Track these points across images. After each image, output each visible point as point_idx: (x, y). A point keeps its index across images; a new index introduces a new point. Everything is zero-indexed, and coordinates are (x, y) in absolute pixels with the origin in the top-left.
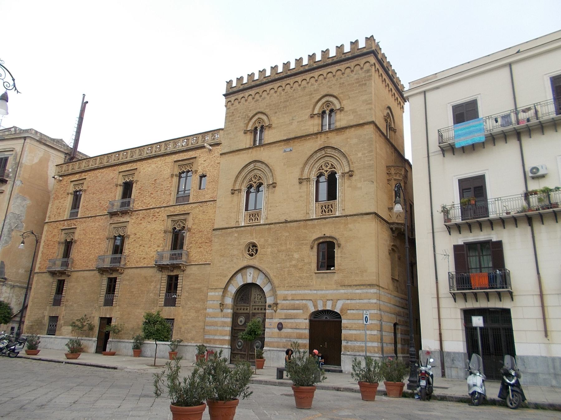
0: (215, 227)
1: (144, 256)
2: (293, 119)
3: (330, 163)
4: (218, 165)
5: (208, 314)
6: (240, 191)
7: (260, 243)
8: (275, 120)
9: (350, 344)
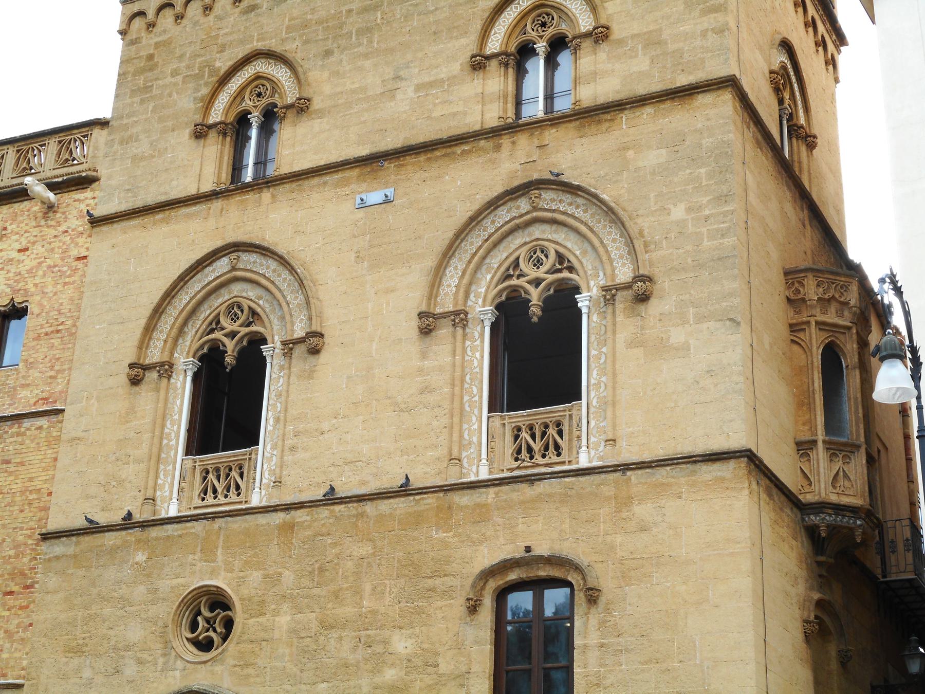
0: (54, 524)
2: (398, 78)
4: (80, 265)
6: (166, 369)
7: (245, 592)
8: (323, 85)
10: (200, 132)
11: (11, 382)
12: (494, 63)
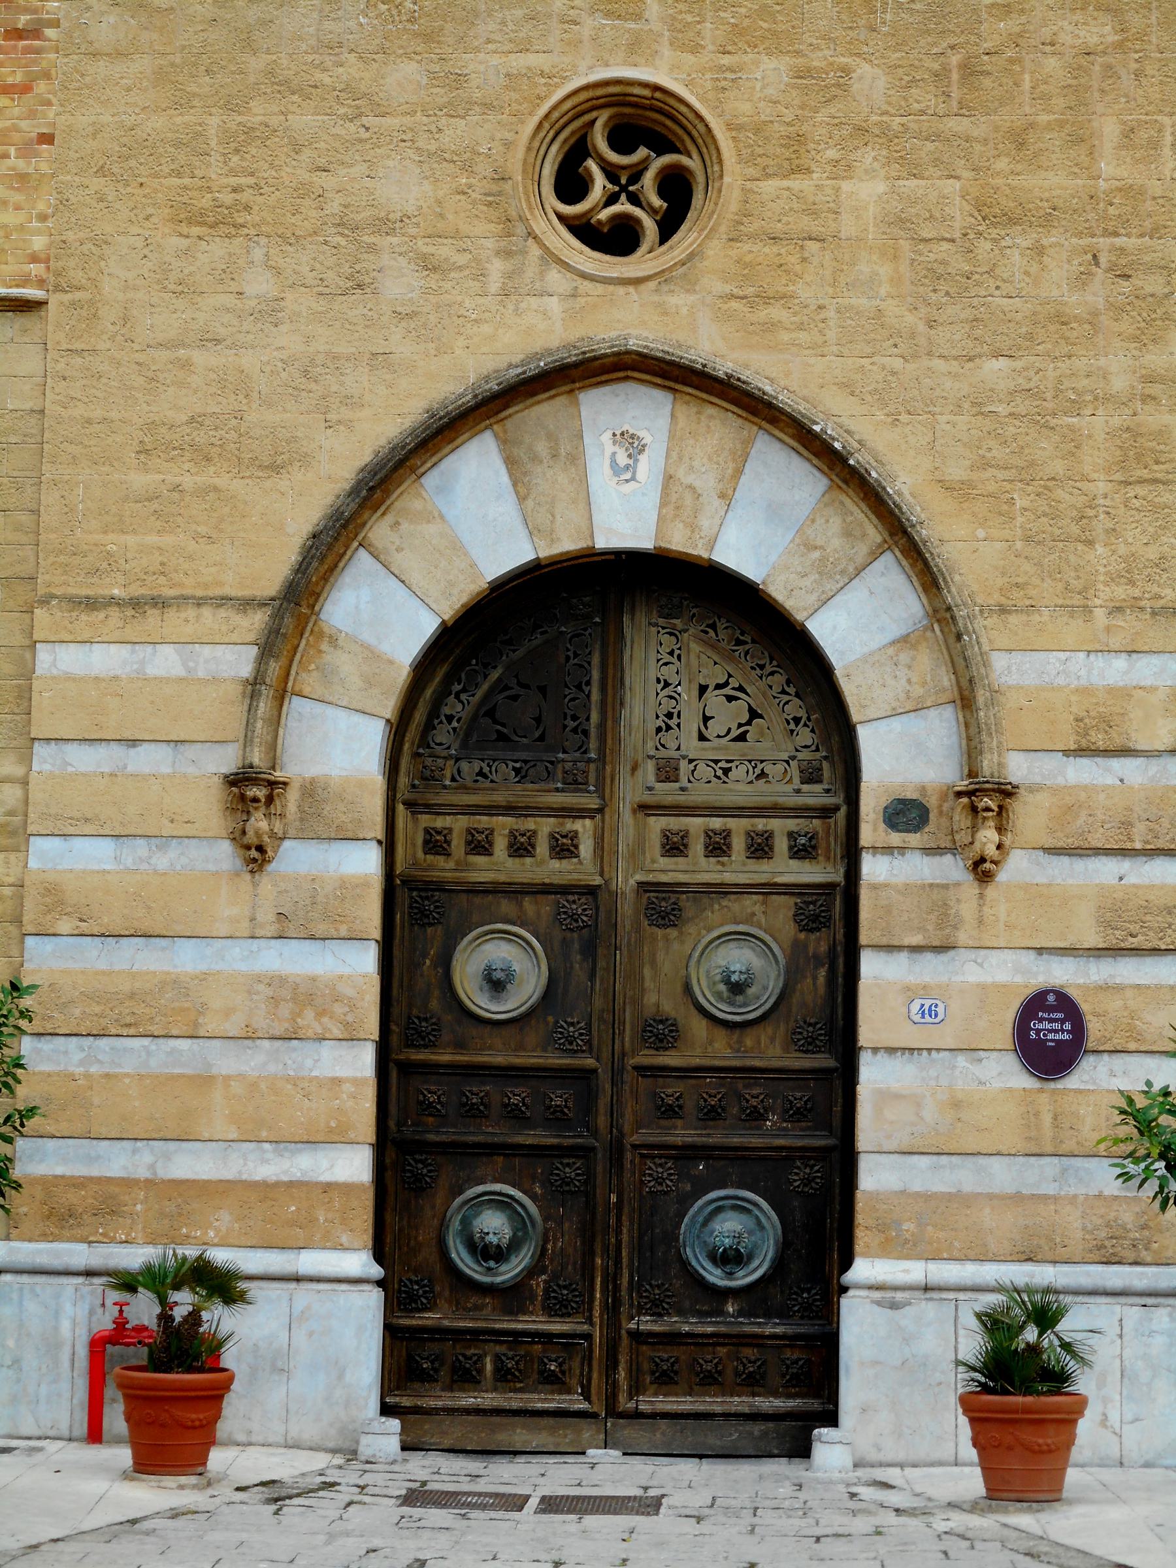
5: (55, 896)
7: (742, 108)
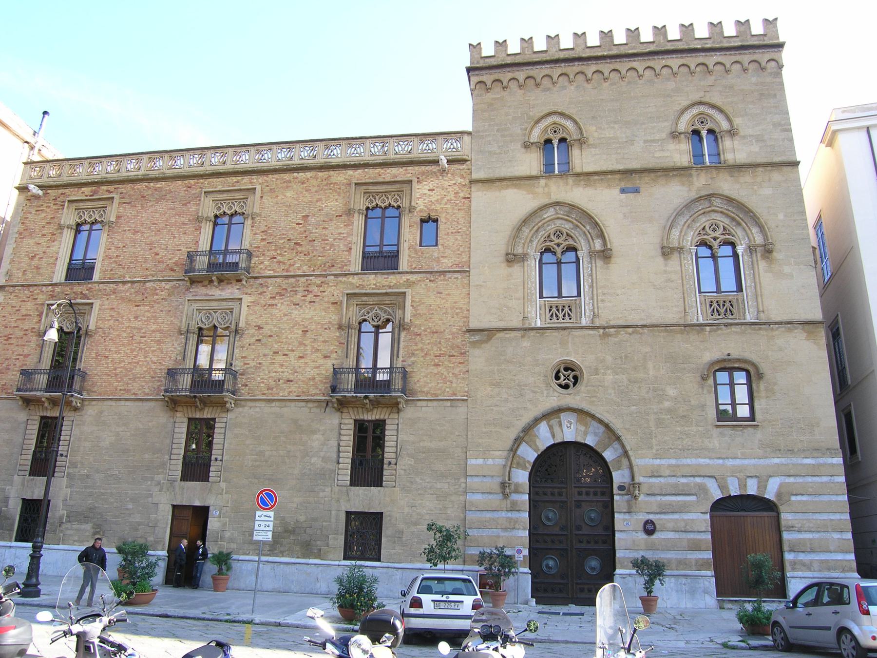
0: (473, 325)
1: (286, 376)
3: (721, 225)
4: (466, 201)
9: (802, 557)
10: (527, 146)
11: (436, 255)
12: (682, 136)
